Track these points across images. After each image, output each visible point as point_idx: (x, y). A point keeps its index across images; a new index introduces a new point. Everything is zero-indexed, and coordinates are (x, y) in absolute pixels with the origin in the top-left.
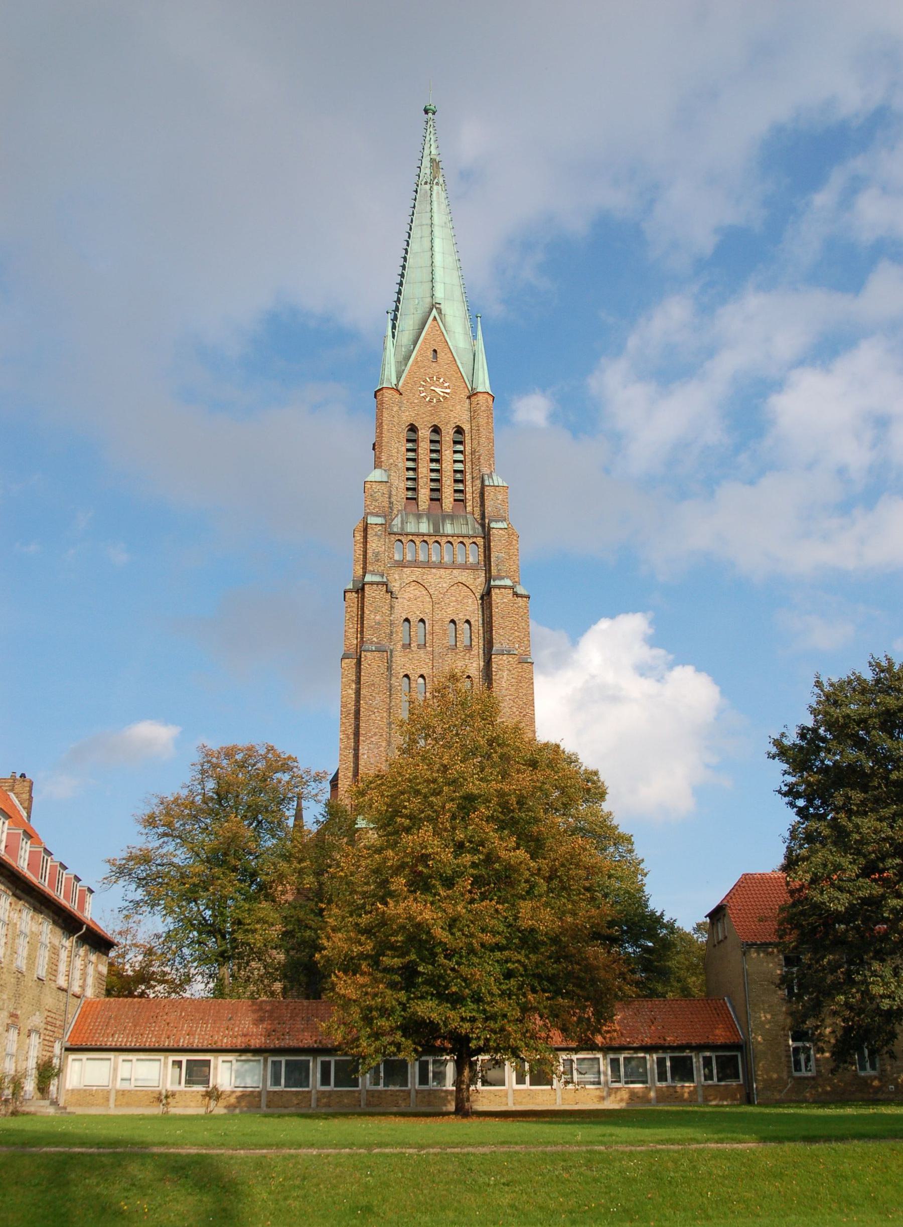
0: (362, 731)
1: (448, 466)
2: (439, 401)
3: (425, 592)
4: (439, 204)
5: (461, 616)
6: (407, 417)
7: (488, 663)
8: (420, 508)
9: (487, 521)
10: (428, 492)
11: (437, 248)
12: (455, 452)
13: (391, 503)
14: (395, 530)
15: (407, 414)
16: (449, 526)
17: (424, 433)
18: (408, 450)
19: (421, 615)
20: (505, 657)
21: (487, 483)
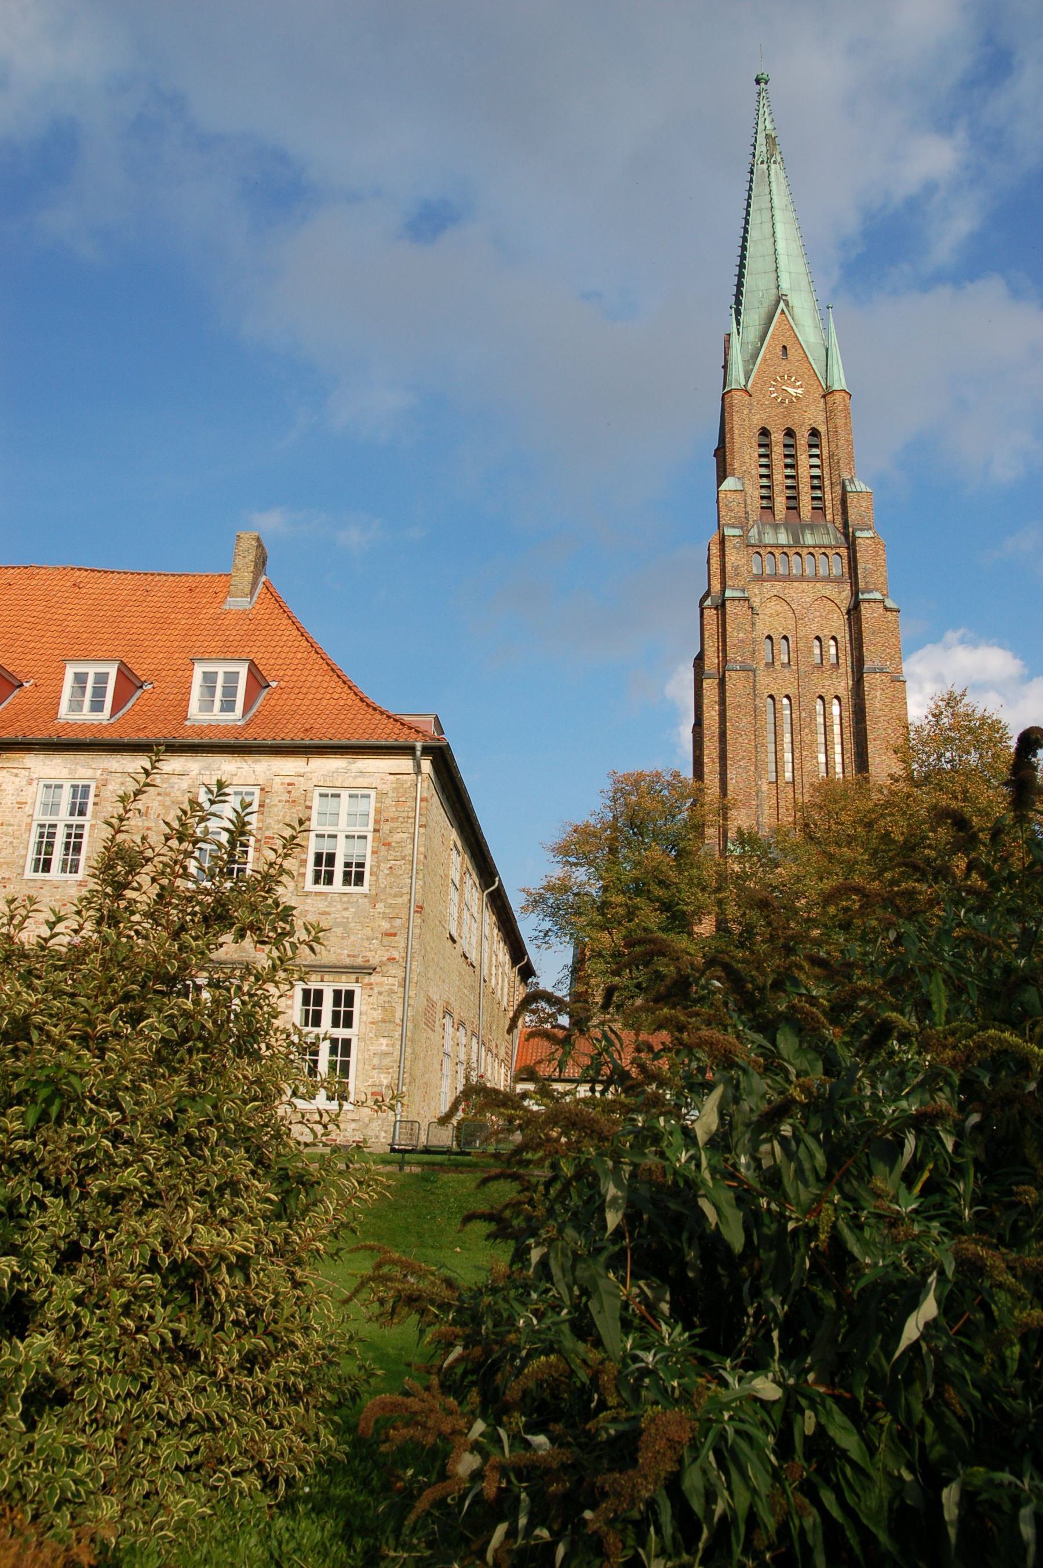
0: (729, 755)
1: (804, 472)
2: (791, 401)
3: (787, 608)
4: (777, 185)
5: (826, 632)
6: (758, 420)
8: (777, 518)
9: (851, 530)
10: (784, 501)
11: (779, 235)
12: (811, 456)
13: (746, 513)
14: (753, 542)
15: (758, 416)
16: (809, 536)
17: (777, 437)
18: (761, 456)
19: (784, 633)
20: (877, 676)
21: (849, 489)
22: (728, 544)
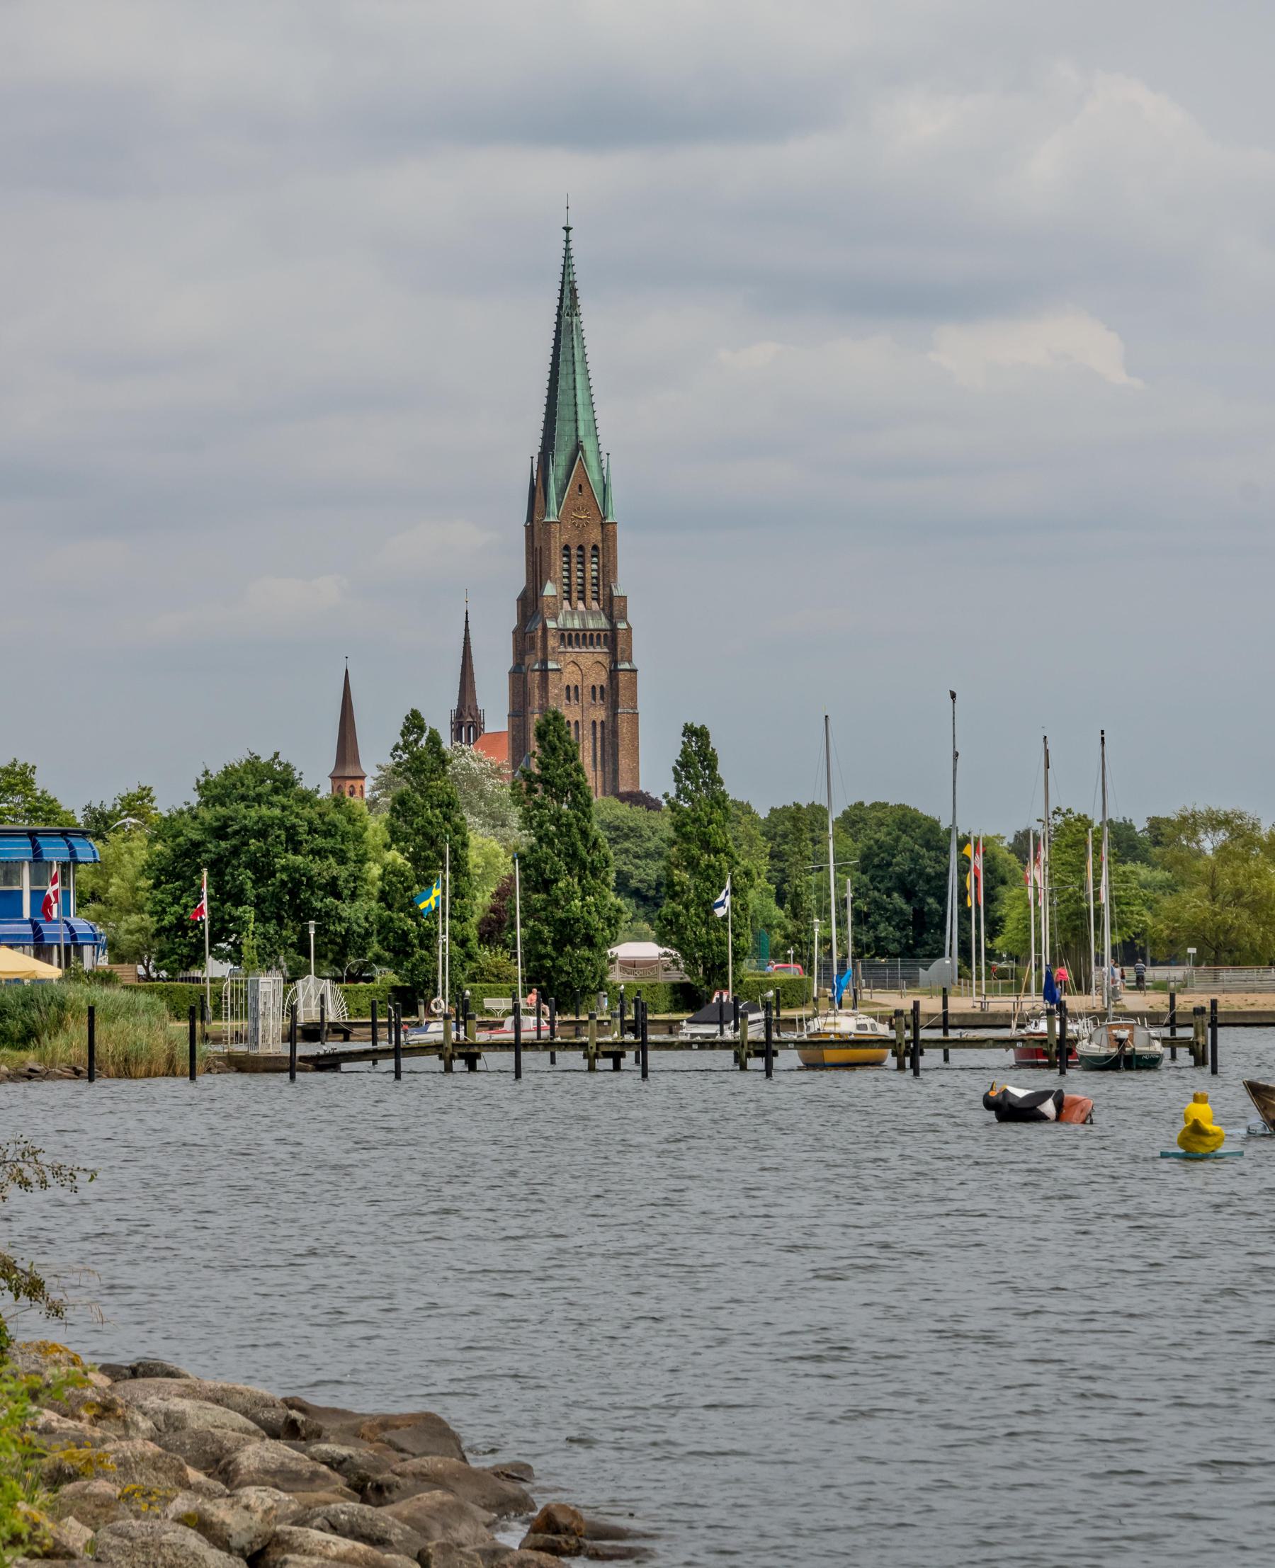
6: (565, 538)
7: (615, 715)
22: (549, 634)
